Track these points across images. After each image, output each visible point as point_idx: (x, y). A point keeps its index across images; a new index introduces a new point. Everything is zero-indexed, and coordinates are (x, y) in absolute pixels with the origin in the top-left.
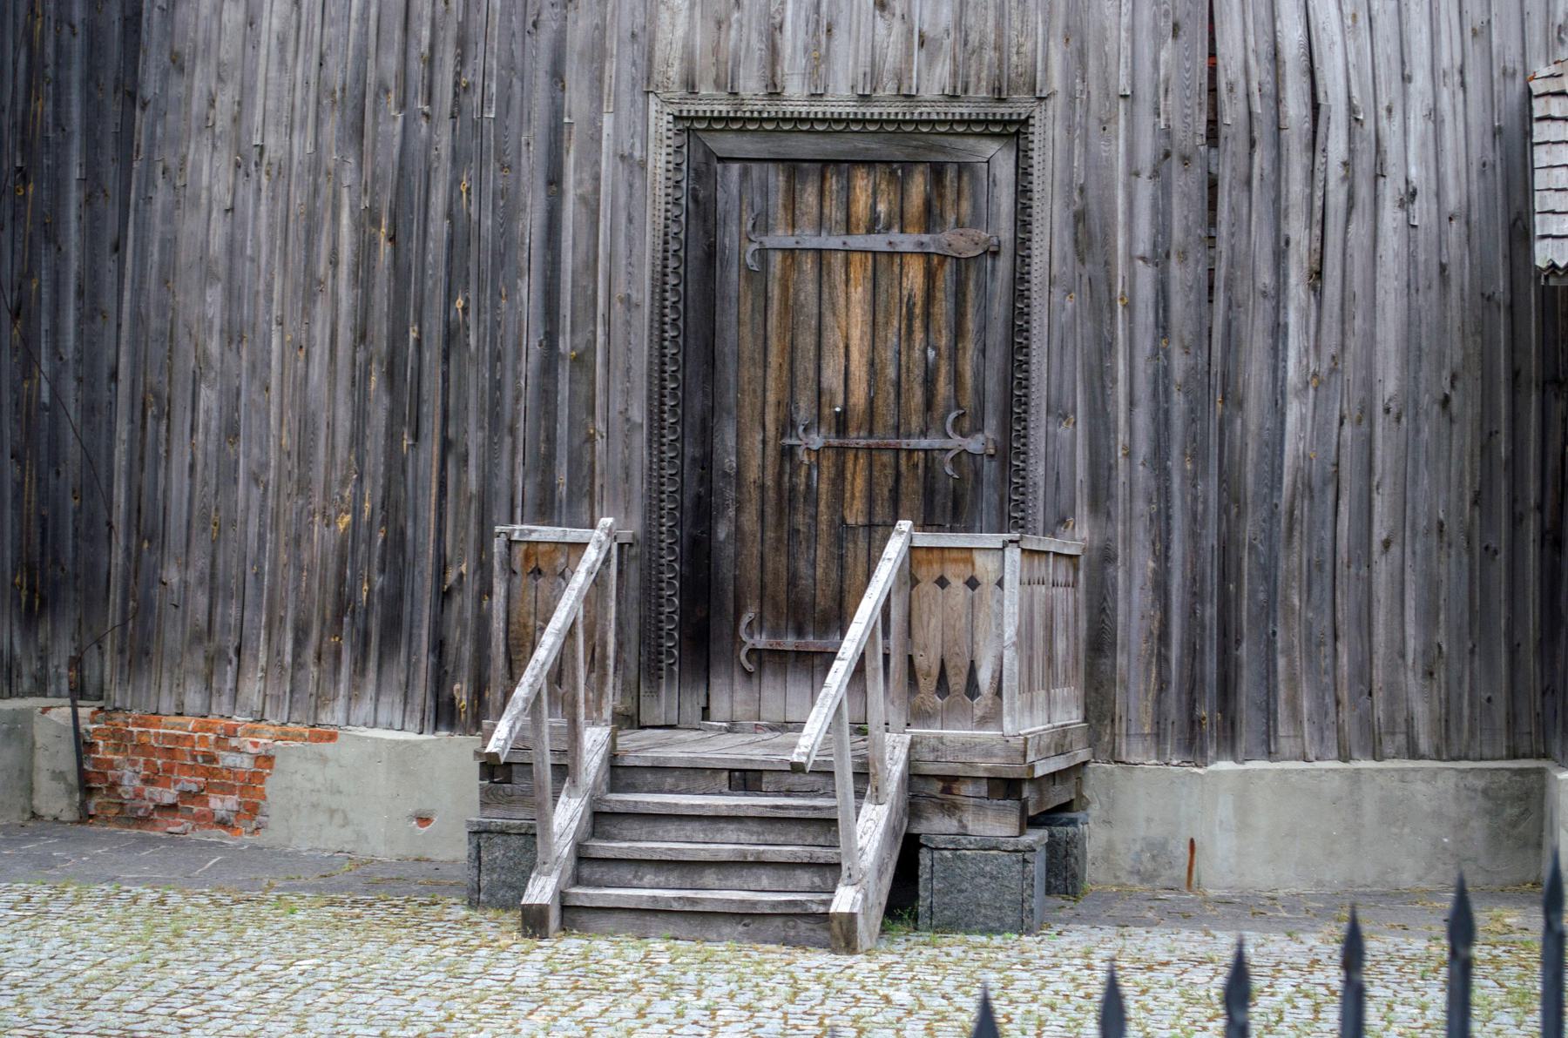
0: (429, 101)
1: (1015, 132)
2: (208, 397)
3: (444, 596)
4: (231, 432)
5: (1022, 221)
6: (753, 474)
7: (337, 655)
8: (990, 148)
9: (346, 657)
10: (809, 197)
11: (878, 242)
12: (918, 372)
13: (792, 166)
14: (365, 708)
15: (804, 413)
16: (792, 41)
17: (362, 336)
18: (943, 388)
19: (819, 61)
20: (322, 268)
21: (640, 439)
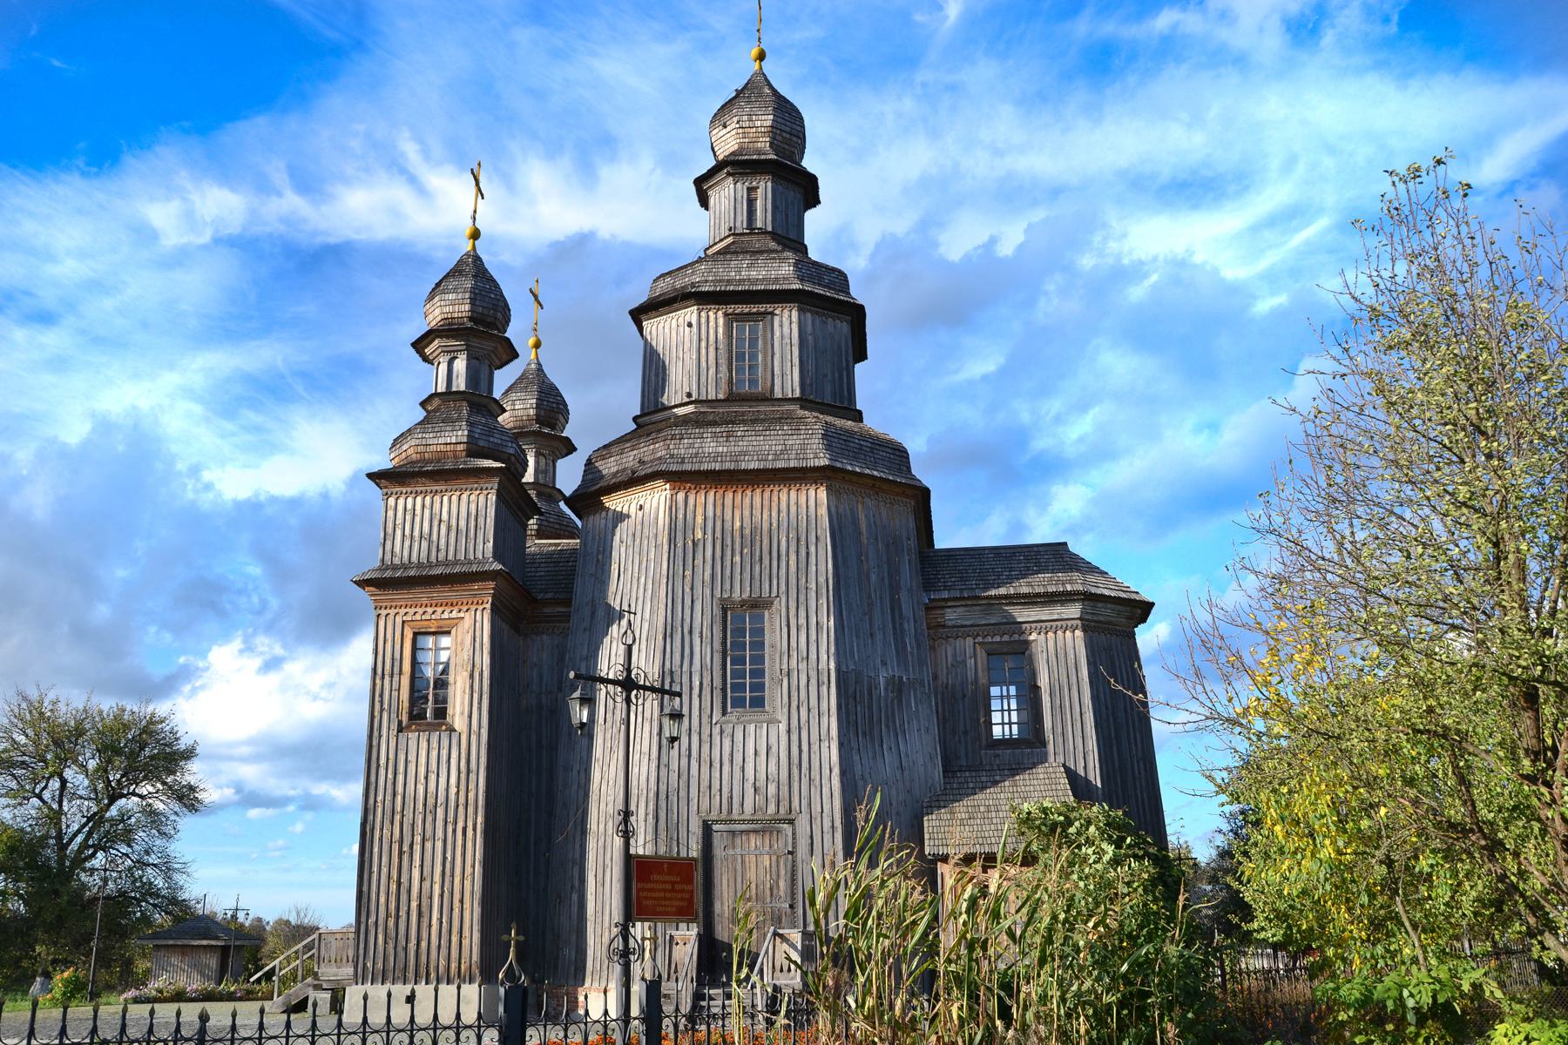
1: (791, 822)
5: (794, 844)
6: (726, 915)
8: (785, 826)
10: (738, 841)
12: (768, 886)
18: (775, 891)
20: (608, 861)
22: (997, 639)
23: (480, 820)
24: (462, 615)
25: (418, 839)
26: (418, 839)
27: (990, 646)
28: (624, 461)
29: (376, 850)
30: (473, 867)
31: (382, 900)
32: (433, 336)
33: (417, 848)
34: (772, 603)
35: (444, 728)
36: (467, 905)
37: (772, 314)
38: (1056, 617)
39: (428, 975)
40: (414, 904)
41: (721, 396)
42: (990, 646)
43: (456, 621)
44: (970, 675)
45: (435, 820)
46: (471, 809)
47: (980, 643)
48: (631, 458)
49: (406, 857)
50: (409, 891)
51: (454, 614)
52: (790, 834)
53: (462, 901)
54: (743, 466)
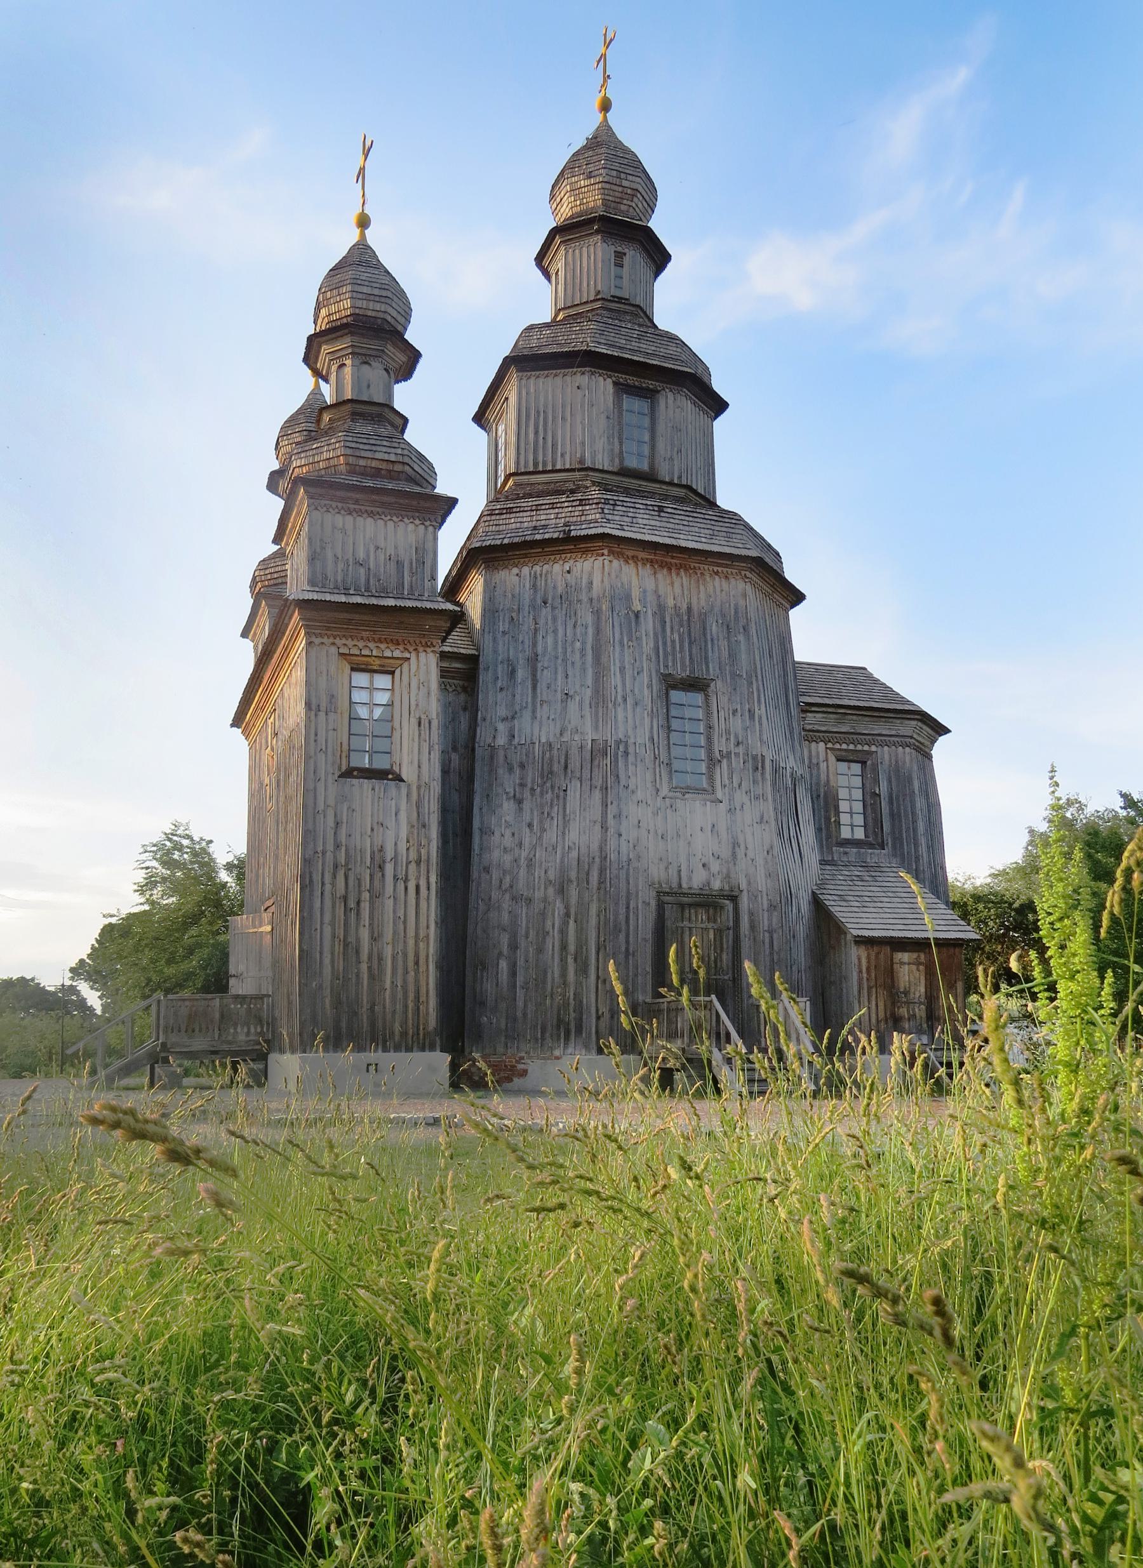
0: (588, 883)
1: (734, 899)
2: (503, 964)
3: (598, 1018)
4: (513, 974)
7: (559, 1036)
8: (727, 902)
9: (562, 1035)
11: (703, 926)
13: (682, 906)
14: (570, 1050)
15: (687, 969)
16: (683, 874)
17: (564, 947)
19: (690, 879)
21: (649, 977)
22: (844, 746)
23: (433, 879)
24: (407, 655)
25: (366, 896)
26: (366, 896)
27: (838, 753)
28: (543, 517)
29: (317, 904)
30: (428, 927)
31: (327, 961)
32: (346, 331)
33: (365, 906)
34: (709, 686)
35: (390, 776)
36: (422, 968)
37: (658, 392)
38: (893, 733)
39: (385, 1042)
40: (364, 967)
41: (611, 469)
42: (838, 753)
43: (400, 662)
44: (823, 777)
45: (383, 875)
46: (423, 866)
47: (831, 749)
48: (552, 516)
49: (353, 915)
50: (357, 952)
51: (397, 654)
52: (731, 909)
53: (417, 963)
54: (683, 544)
